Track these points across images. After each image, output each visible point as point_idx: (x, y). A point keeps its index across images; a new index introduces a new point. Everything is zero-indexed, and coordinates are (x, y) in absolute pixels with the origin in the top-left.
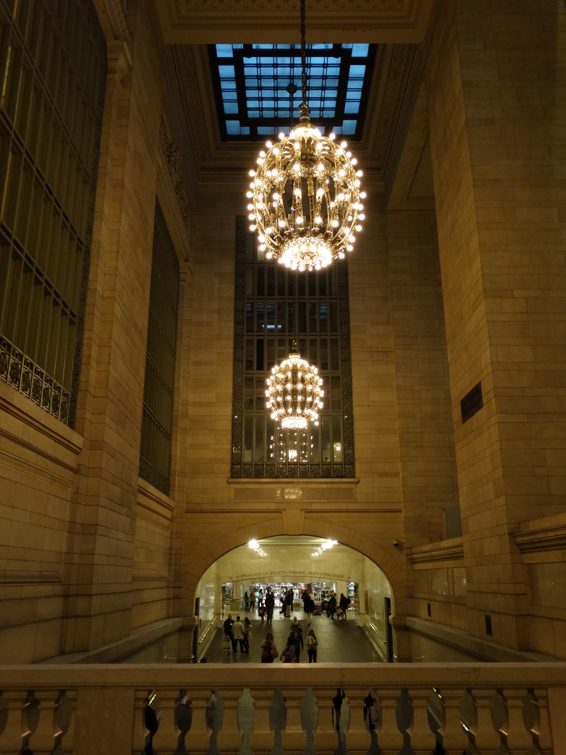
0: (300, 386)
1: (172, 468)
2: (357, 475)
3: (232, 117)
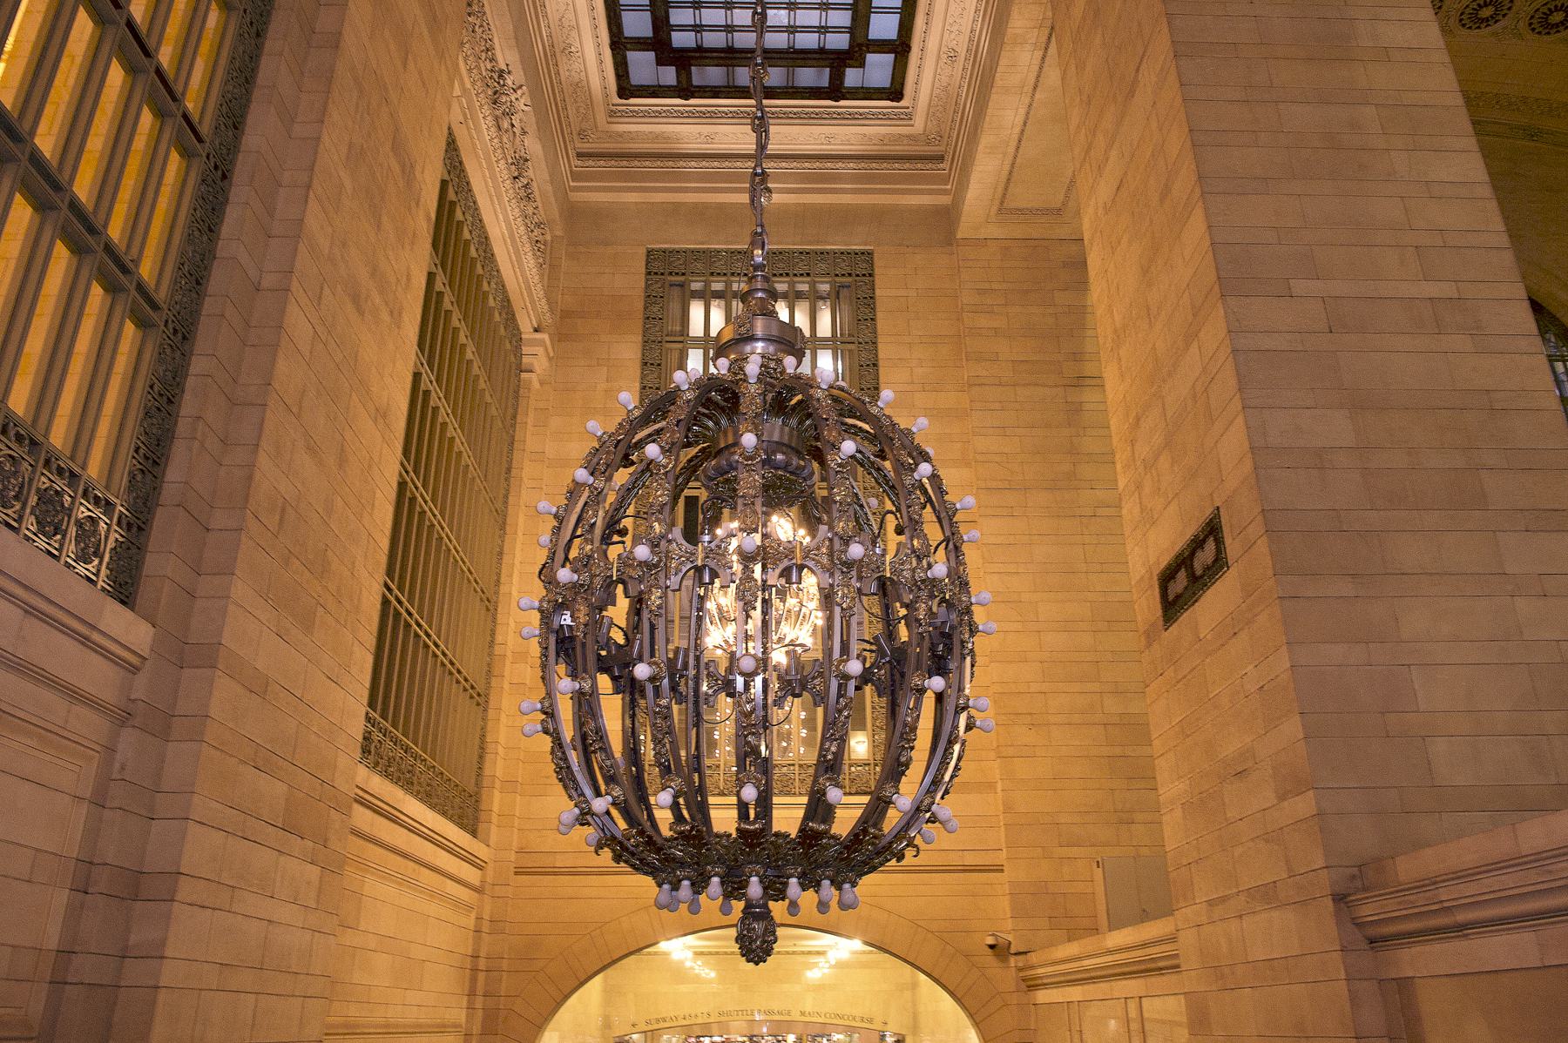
1: (487, 772)
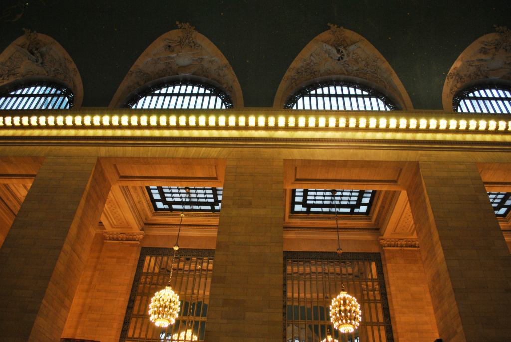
0: (348, 308)
3: (299, 203)
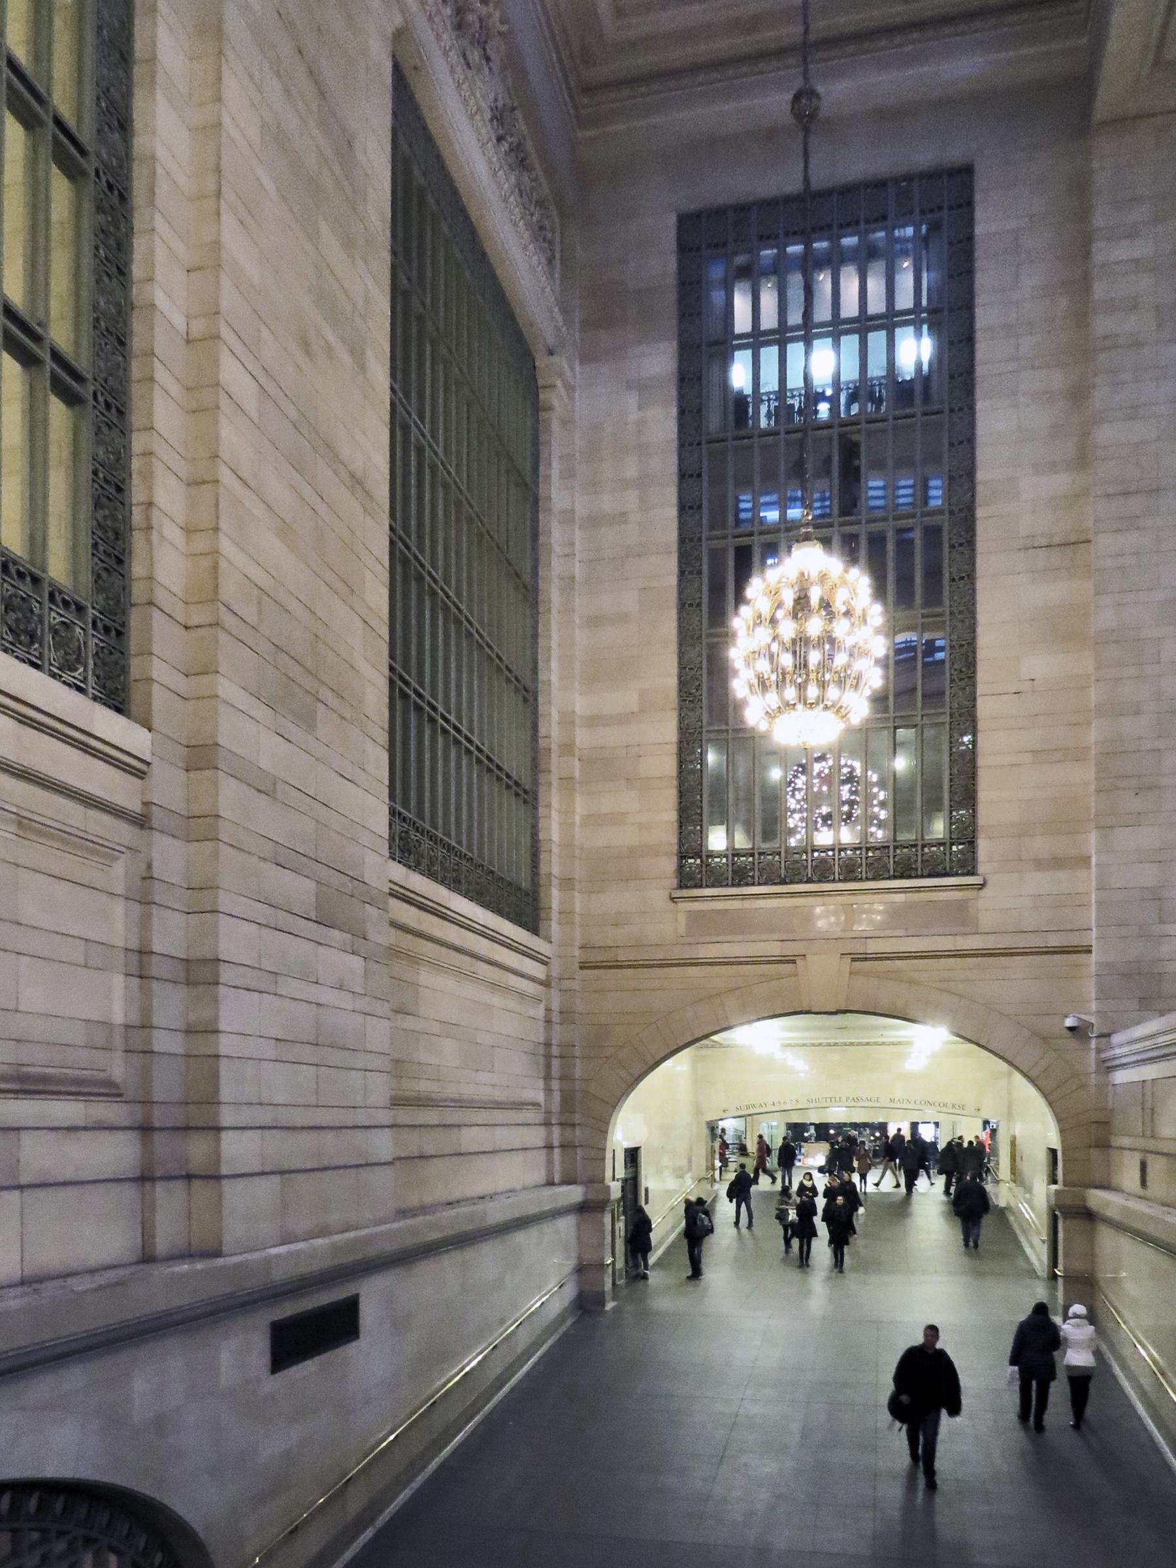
1: (543, 869)
2: (982, 868)
